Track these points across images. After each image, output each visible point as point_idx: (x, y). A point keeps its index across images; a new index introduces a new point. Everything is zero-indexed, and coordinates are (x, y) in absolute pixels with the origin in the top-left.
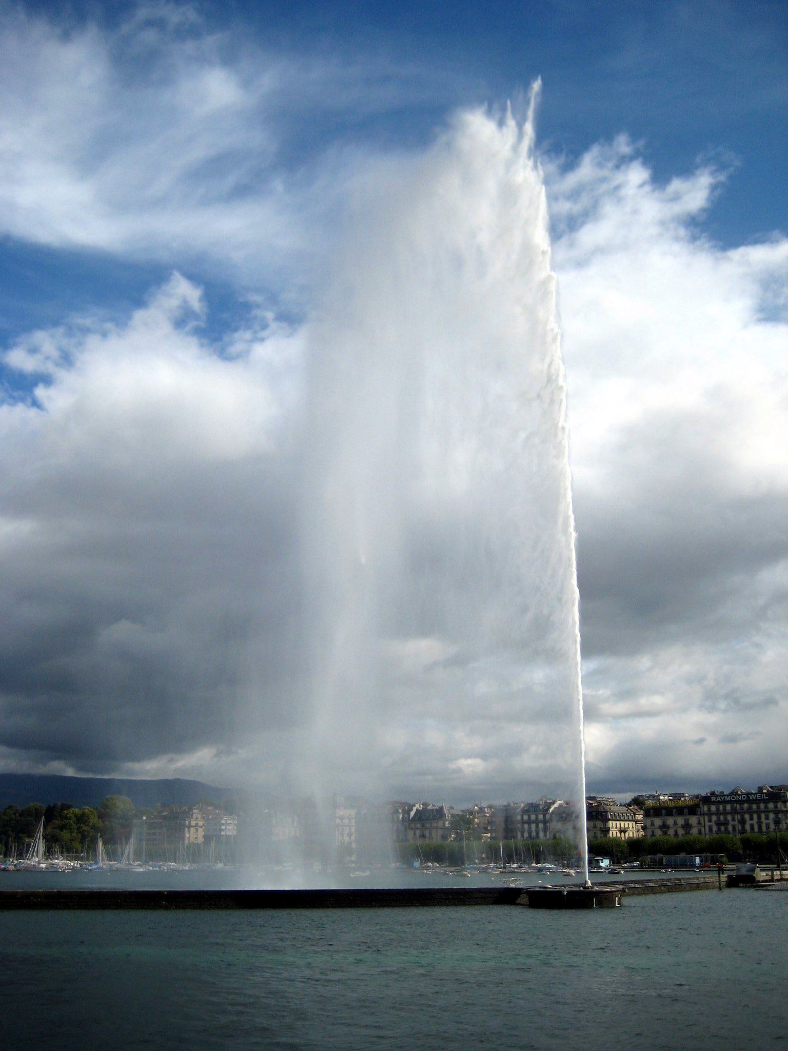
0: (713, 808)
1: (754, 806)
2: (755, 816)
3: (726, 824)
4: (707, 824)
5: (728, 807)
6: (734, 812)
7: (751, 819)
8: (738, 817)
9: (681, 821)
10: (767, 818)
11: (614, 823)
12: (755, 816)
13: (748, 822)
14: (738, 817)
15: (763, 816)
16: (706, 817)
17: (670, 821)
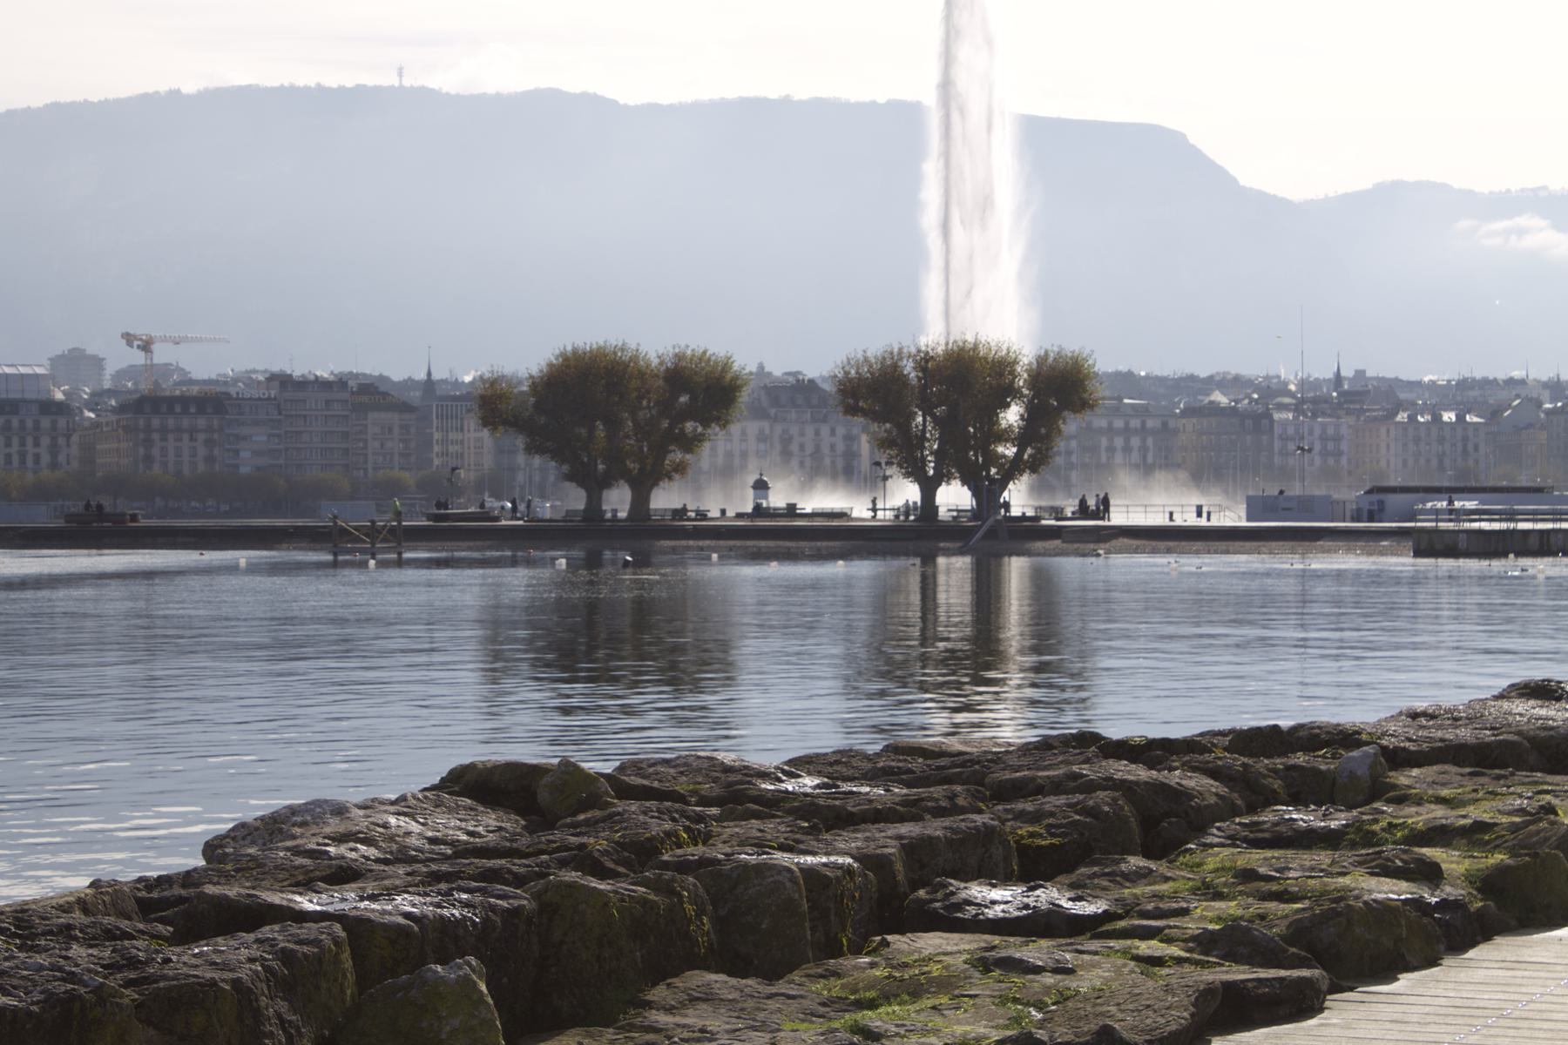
2: (15, 441)
10: (37, 444)
12: (15, 441)
15: (30, 441)
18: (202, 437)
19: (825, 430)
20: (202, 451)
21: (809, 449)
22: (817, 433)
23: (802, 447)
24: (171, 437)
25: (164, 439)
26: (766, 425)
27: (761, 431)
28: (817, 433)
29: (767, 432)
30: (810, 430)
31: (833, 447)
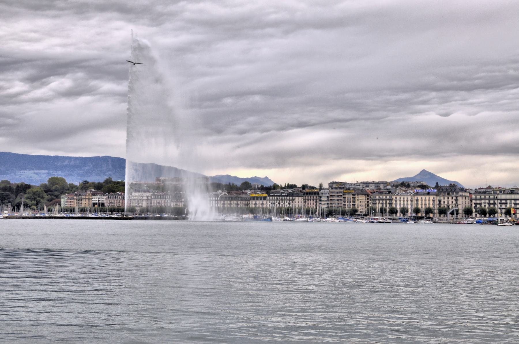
0: (271, 198)
1: (283, 198)
2: (283, 201)
3: (274, 204)
4: (269, 203)
5: (276, 198)
6: (277, 200)
7: (282, 202)
8: (278, 201)
9: (261, 202)
10: (287, 202)
11: (242, 202)
12: (283, 201)
13: (281, 203)
14: (278, 201)
15: (286, 201)
16: (269, 201)
17: (257, 202)
18: (315, 200)
19: (450, 198)
20: (315, 204)
21: (446, 203)
22: (448, 198)
23: (444, 202)
24: (309, 200)
25: (308, 201)
26: (435, 197)
27: (434, 198)
28: (448, 198)
29: (435, 198)
30: (446, 198)
31: (452, 202)
